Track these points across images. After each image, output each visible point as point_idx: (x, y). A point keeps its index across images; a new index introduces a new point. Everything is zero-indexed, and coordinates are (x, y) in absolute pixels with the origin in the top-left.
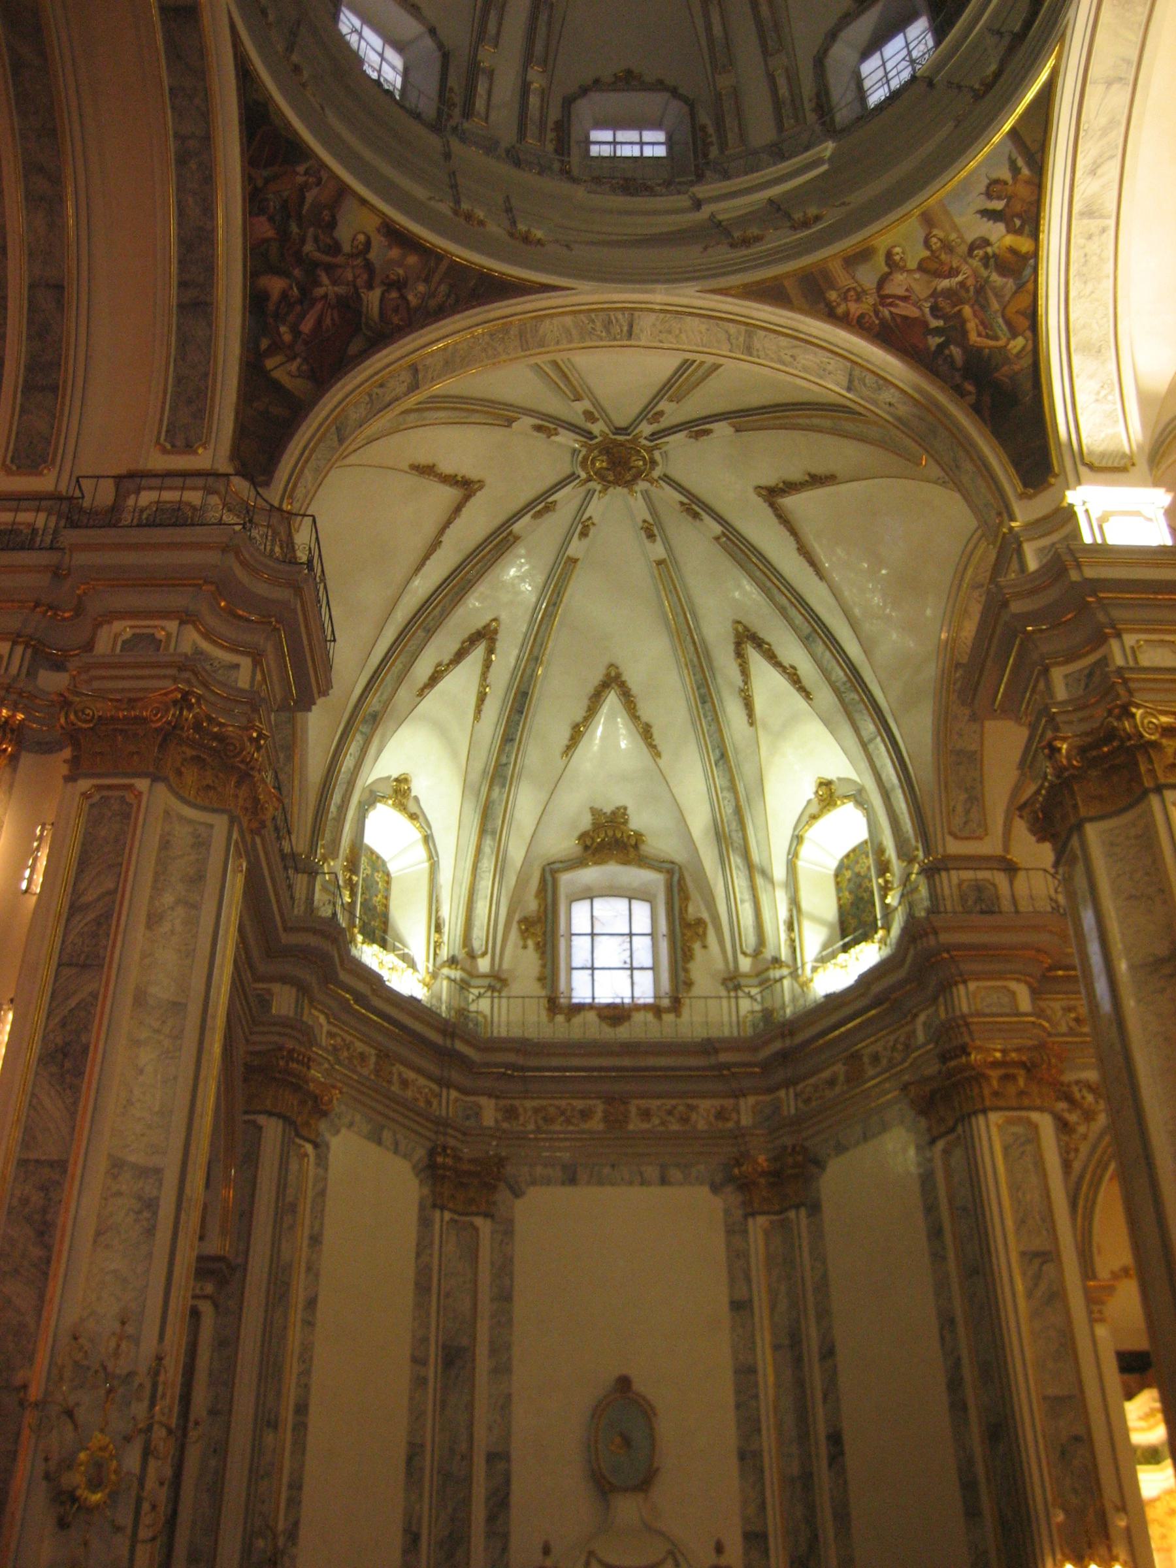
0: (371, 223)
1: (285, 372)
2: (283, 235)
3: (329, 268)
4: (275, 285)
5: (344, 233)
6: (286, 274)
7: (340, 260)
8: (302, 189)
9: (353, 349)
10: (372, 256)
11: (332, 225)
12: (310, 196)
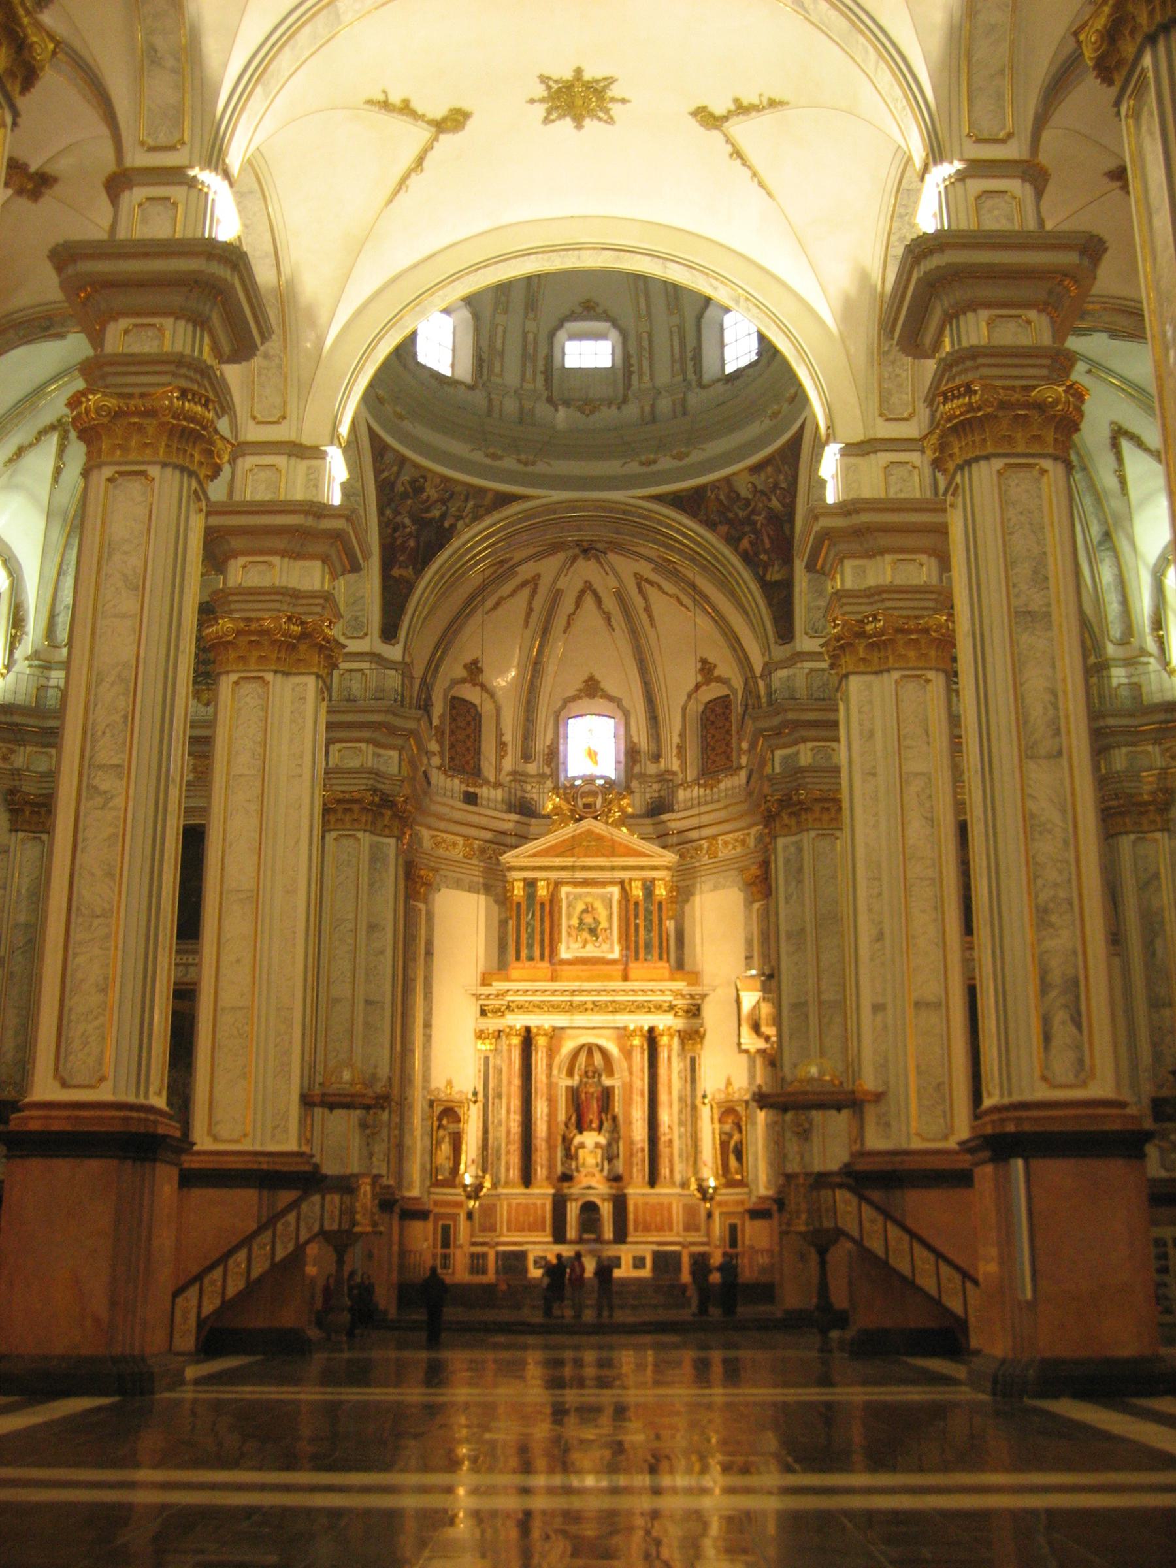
0: (746, 476)
1: (774, 575)
2: (730, 522)
3: (753, 512)
4: (745, 544)
5: (745, 492)
6: (745, 534)
7: (753, 504)
8: (717, 499)
9: (788, 533)
10: (759, 487)
11: (738, 495)
12: (722, 497)
